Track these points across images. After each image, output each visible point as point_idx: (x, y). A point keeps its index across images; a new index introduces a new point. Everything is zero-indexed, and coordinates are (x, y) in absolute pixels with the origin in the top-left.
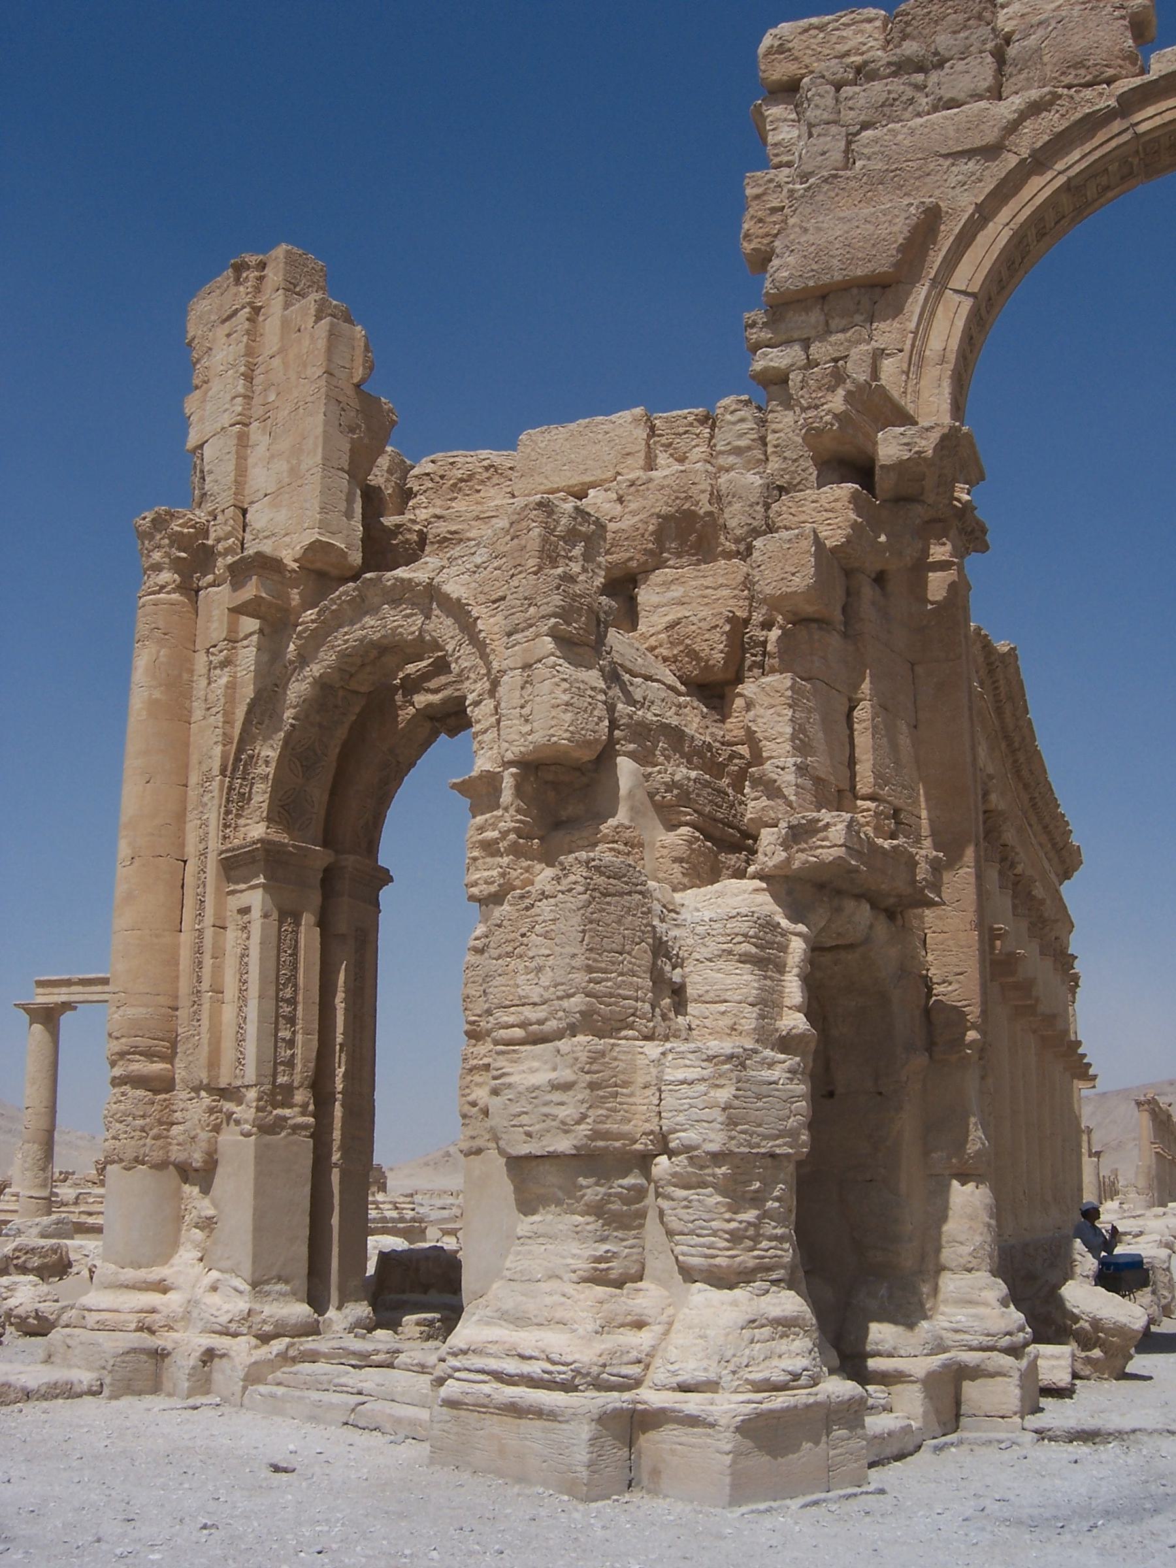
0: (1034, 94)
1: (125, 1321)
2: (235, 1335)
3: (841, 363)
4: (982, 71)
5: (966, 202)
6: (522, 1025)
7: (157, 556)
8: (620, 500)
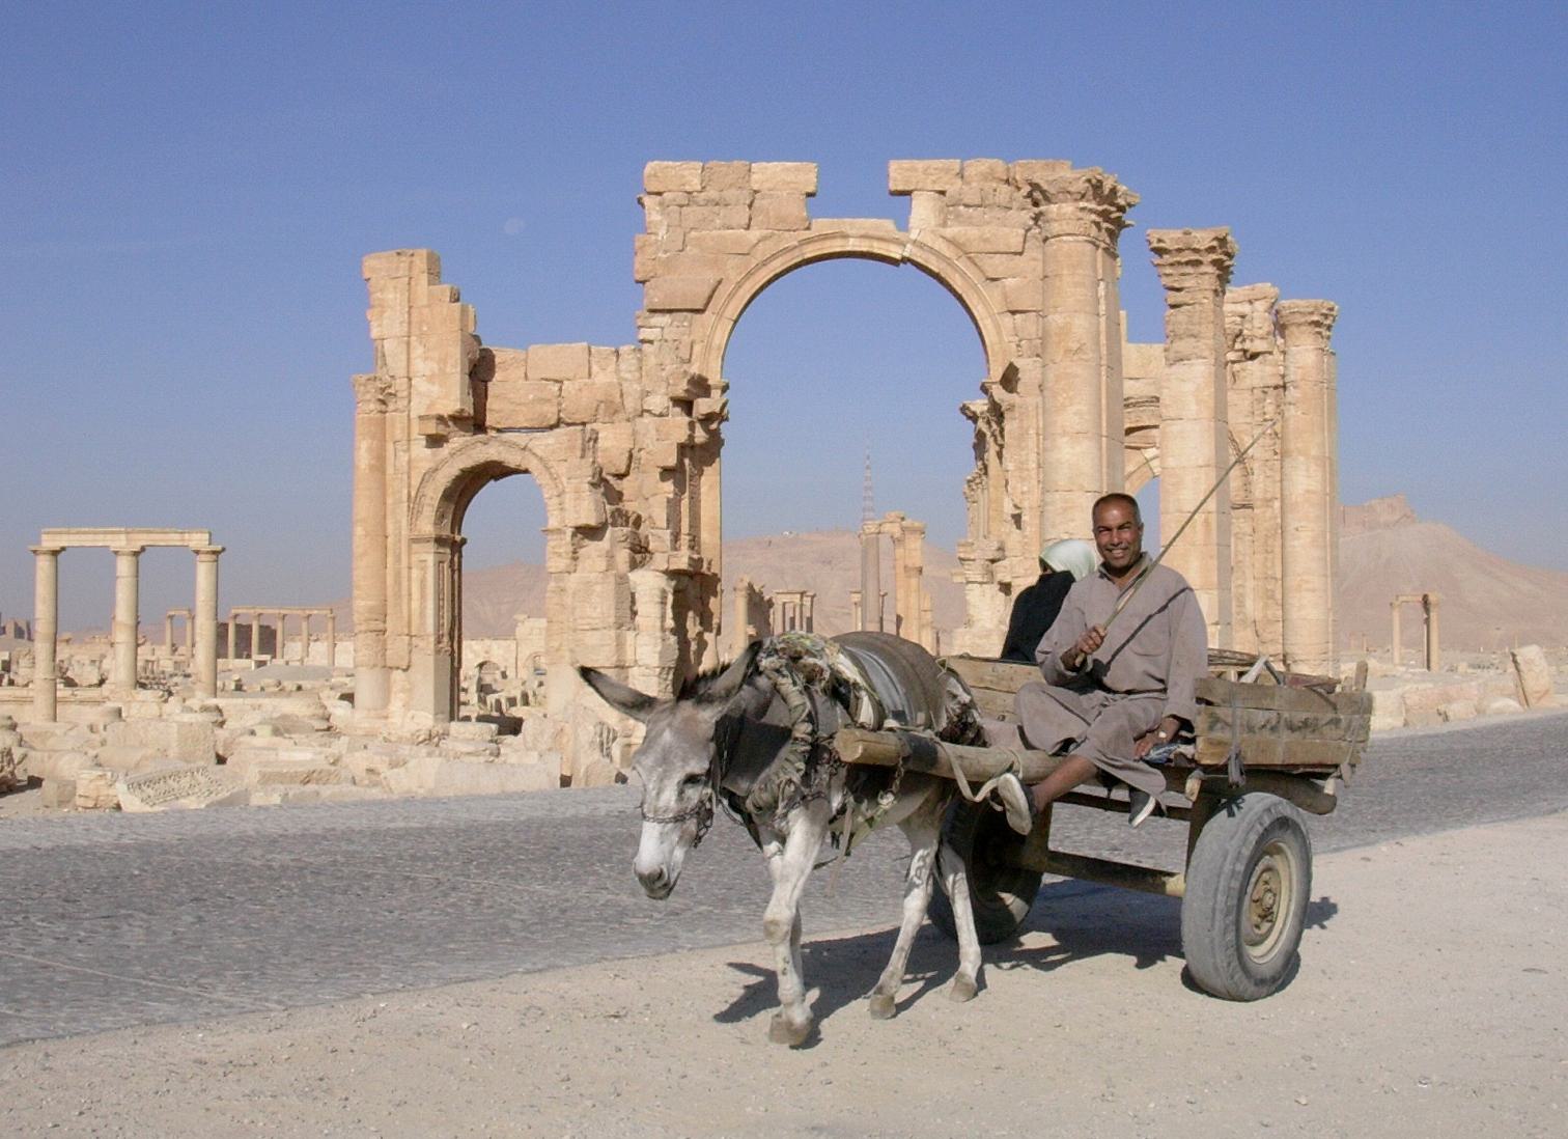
0: (765, 232)
3: (677, 343)
4: (742, 215)
5: (734, 276)
6: (589, 624)
7: (368, 397)
8: (580, 390)
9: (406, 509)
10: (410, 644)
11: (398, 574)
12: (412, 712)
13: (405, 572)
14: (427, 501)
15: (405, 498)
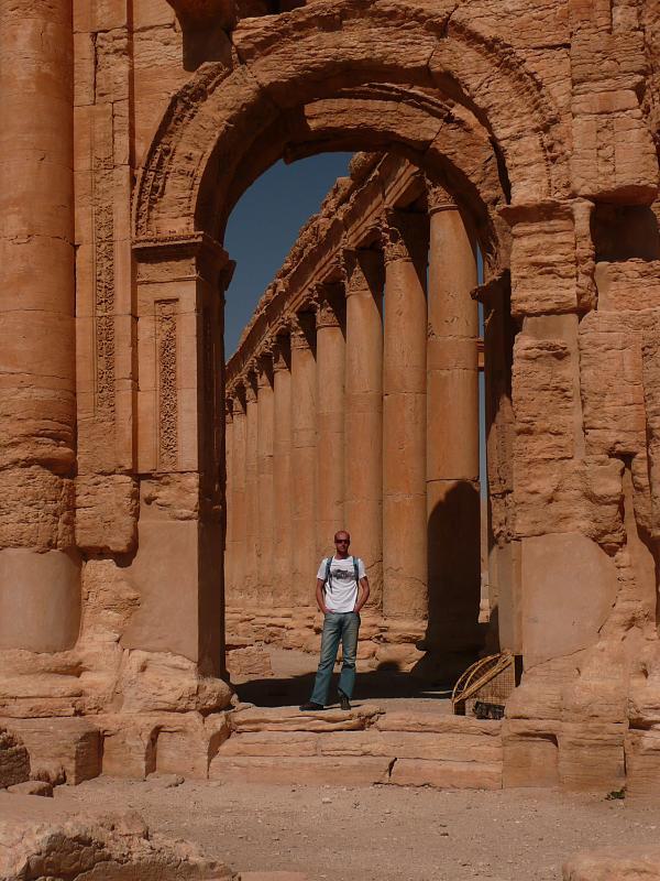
1: (63, 707)
2: (184, 711)
9: (125, 181)
10: (135, 496)
11: (105, 336)
12: (139, 656)
13: (123, 325)
14: (178, 163)
15: (122, 156)
